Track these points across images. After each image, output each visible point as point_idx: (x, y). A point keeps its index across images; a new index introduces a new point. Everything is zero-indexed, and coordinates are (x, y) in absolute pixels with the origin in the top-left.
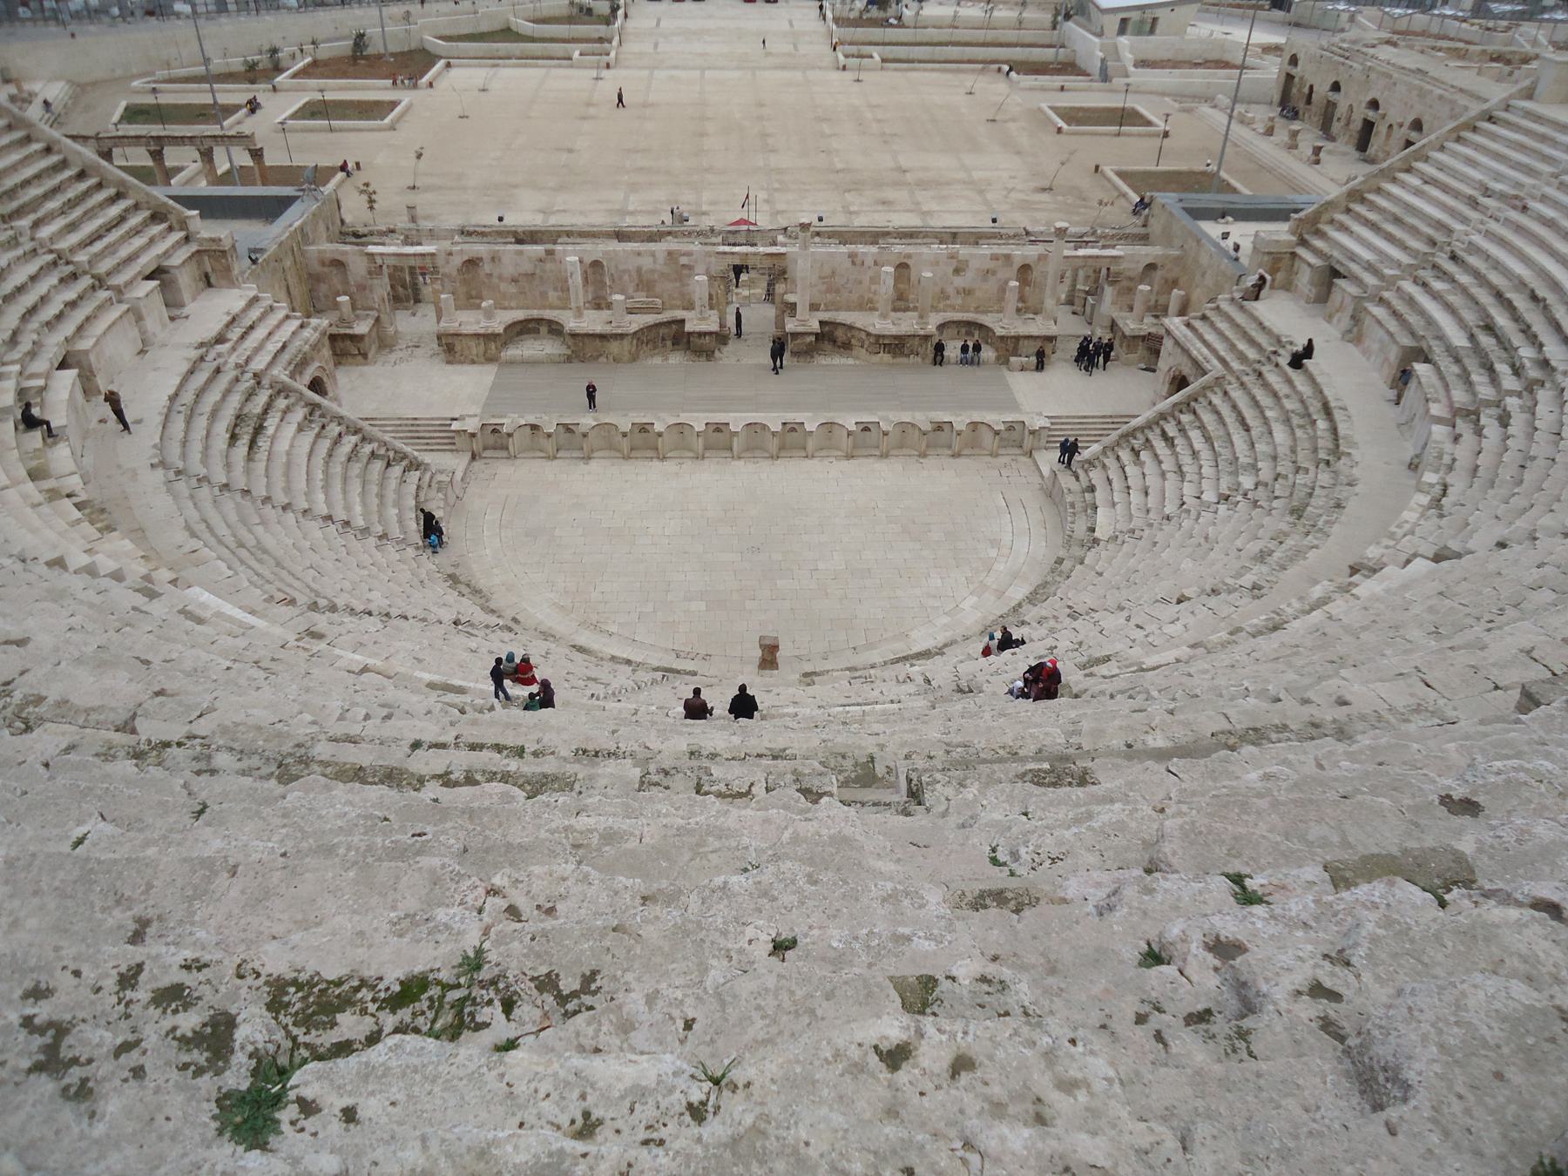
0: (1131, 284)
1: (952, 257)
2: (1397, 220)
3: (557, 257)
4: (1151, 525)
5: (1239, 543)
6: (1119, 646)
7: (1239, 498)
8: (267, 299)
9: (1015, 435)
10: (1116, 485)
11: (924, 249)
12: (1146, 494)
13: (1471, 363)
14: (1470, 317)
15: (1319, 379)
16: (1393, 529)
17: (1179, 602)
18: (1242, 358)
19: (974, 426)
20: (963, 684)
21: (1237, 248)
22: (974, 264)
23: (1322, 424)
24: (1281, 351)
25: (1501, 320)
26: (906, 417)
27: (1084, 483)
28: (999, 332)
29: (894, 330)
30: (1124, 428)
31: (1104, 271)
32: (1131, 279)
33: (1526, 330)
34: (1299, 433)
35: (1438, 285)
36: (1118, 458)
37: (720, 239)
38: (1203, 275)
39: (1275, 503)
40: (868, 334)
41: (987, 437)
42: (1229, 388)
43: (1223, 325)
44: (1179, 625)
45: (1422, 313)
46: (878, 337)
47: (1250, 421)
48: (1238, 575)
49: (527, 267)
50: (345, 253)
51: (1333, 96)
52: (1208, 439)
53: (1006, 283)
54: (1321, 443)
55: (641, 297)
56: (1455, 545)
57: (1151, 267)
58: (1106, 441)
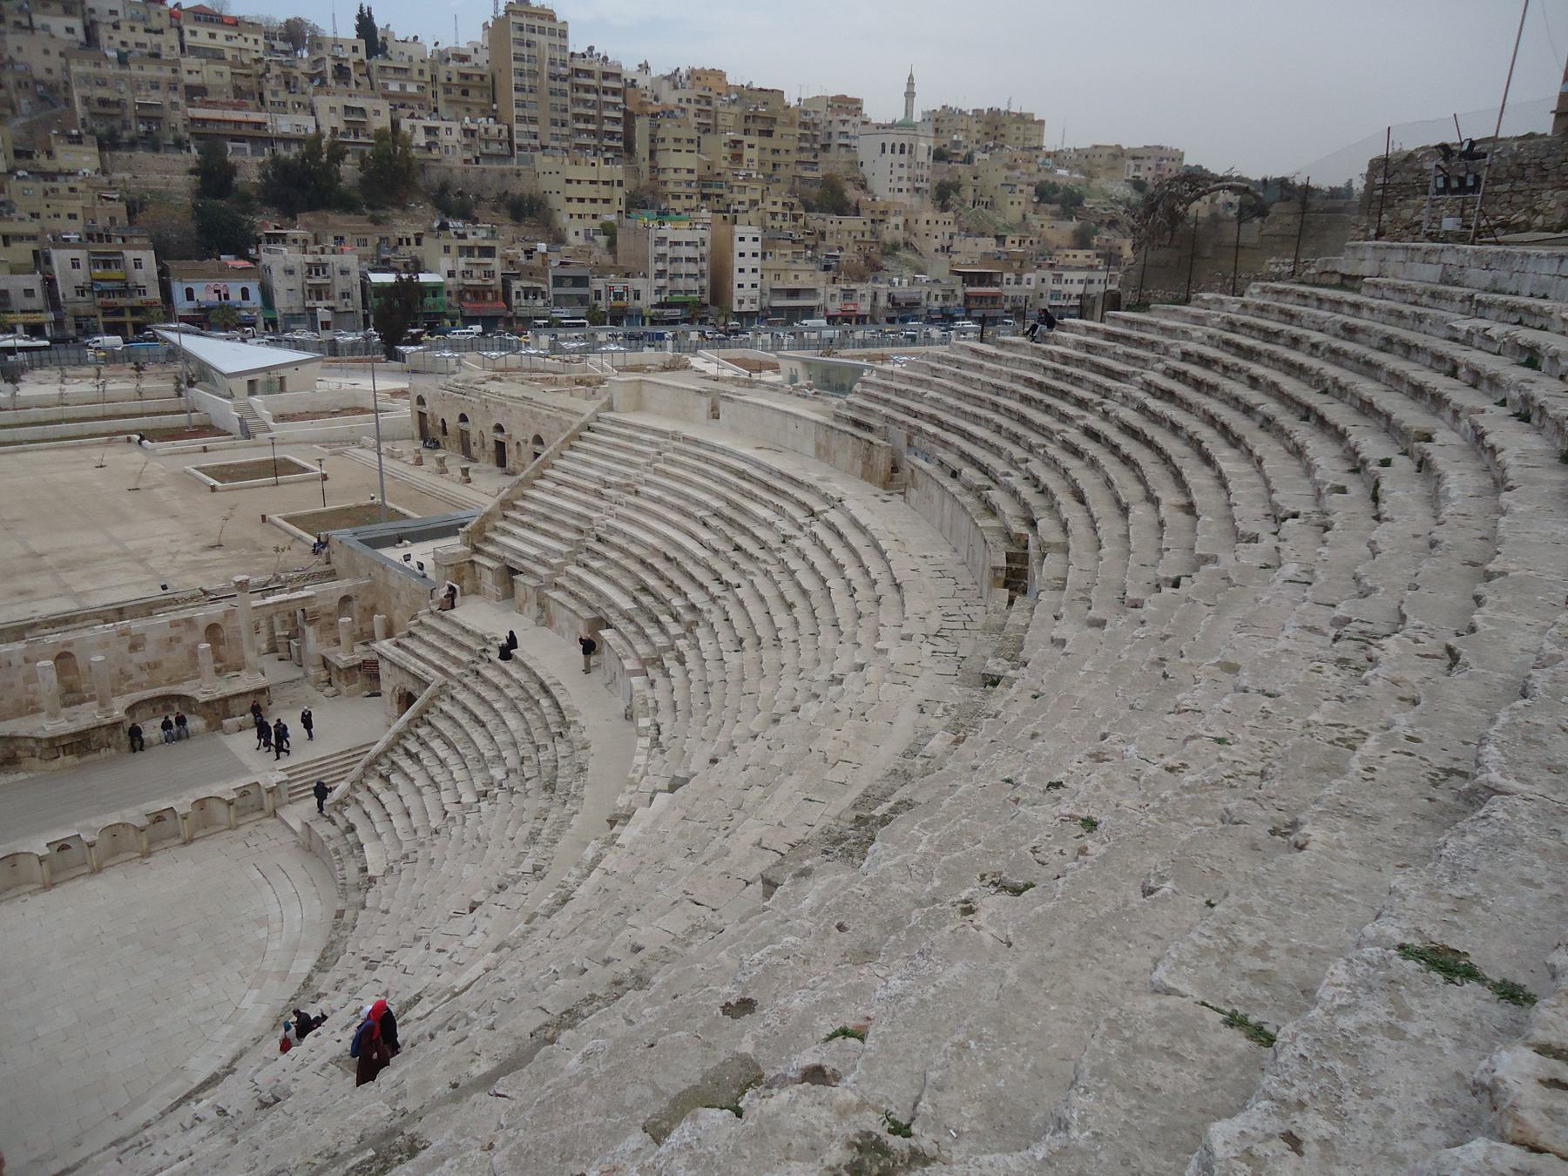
0: (331, 619)
1: (123, 634)
2: (547, 519)
4: (422, 844)
5: (509, 833)
6: (426, 980)
7: (496, 790)
9: (252, 799)
10: (374, 817)
11: (86, 633)
12: (409, 815)
13: (641, 620)
14: (627, 583)
15: (529, 664)
16: (631, 775)
17: (472, 910)
18: (457, 662)
19: (201, 803)
20: (267, 1096)
21: (421, 566)
22: (152, 636)
23: (545, 702)
24: (489, 648)
25: (652, 581)
26: (113, 819)
27: (342, 825)
28: (202, 698)
29: (72, 728)
30: (366, 757)
31: (299, 613)
32: (329, 615)
33: (670, 585)
34: (528, 715)
35: (596, 564)
36: (369, 789)
39: (528, 785)
40: (38, 740)
41: (220, 812)
42: (454, 692)
43: (430, 638)
44: (478, 934)
45: (591, 588)
46: (52, 740)
47: (482, 717)
48: (518, 863)
51: (463, 426)
52: (450, 745)
53: (195, 646)
54: (549, 719)
56: (681, 774)
57: (346, 600)
58: (352, 776)
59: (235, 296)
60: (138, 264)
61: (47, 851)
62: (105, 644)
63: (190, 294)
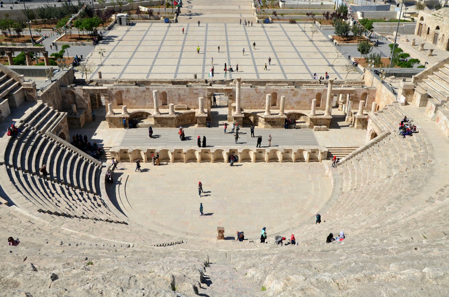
3: (150, 90)
8: (46, 105)
30: (354, 152)
37: (209, 84)
38: (383, 97)
44: (365, 223)
51: (438, 31)
55: (180, 105)
58: (347, 157)
62: (286, 92)
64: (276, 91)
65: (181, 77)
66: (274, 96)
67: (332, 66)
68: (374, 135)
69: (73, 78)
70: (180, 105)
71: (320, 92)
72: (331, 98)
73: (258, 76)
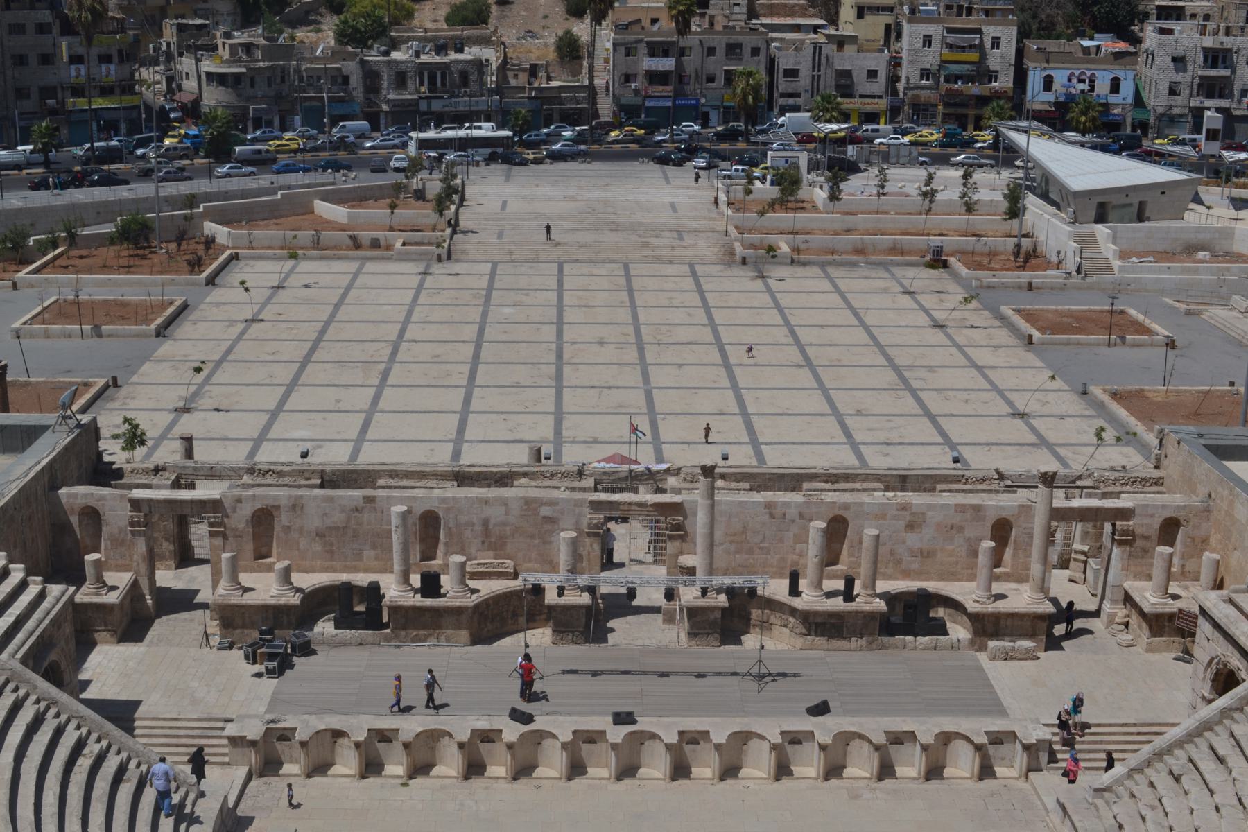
11: (865, 498)
30: (1159, 742)
32: (1146, 538)
37: (589, 482)
49: (338, 518)
50: (102, 498)
55: (488, 560)
59: (1102, 87)
60: (996, 42)
61: (779, 740)
62: (880, 515)
63: (1048, 84)
64: (841, 513)
65: (475, 457)
66: (837, 529)
67: (1023, 415)
68: (1222, 678)
69: (94, 457)
70: (488, 560)
71: (1004, 515)
72: (1050, 535)
73: (759, 455)
